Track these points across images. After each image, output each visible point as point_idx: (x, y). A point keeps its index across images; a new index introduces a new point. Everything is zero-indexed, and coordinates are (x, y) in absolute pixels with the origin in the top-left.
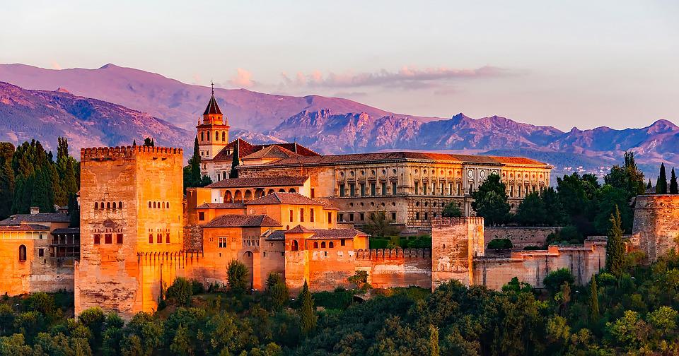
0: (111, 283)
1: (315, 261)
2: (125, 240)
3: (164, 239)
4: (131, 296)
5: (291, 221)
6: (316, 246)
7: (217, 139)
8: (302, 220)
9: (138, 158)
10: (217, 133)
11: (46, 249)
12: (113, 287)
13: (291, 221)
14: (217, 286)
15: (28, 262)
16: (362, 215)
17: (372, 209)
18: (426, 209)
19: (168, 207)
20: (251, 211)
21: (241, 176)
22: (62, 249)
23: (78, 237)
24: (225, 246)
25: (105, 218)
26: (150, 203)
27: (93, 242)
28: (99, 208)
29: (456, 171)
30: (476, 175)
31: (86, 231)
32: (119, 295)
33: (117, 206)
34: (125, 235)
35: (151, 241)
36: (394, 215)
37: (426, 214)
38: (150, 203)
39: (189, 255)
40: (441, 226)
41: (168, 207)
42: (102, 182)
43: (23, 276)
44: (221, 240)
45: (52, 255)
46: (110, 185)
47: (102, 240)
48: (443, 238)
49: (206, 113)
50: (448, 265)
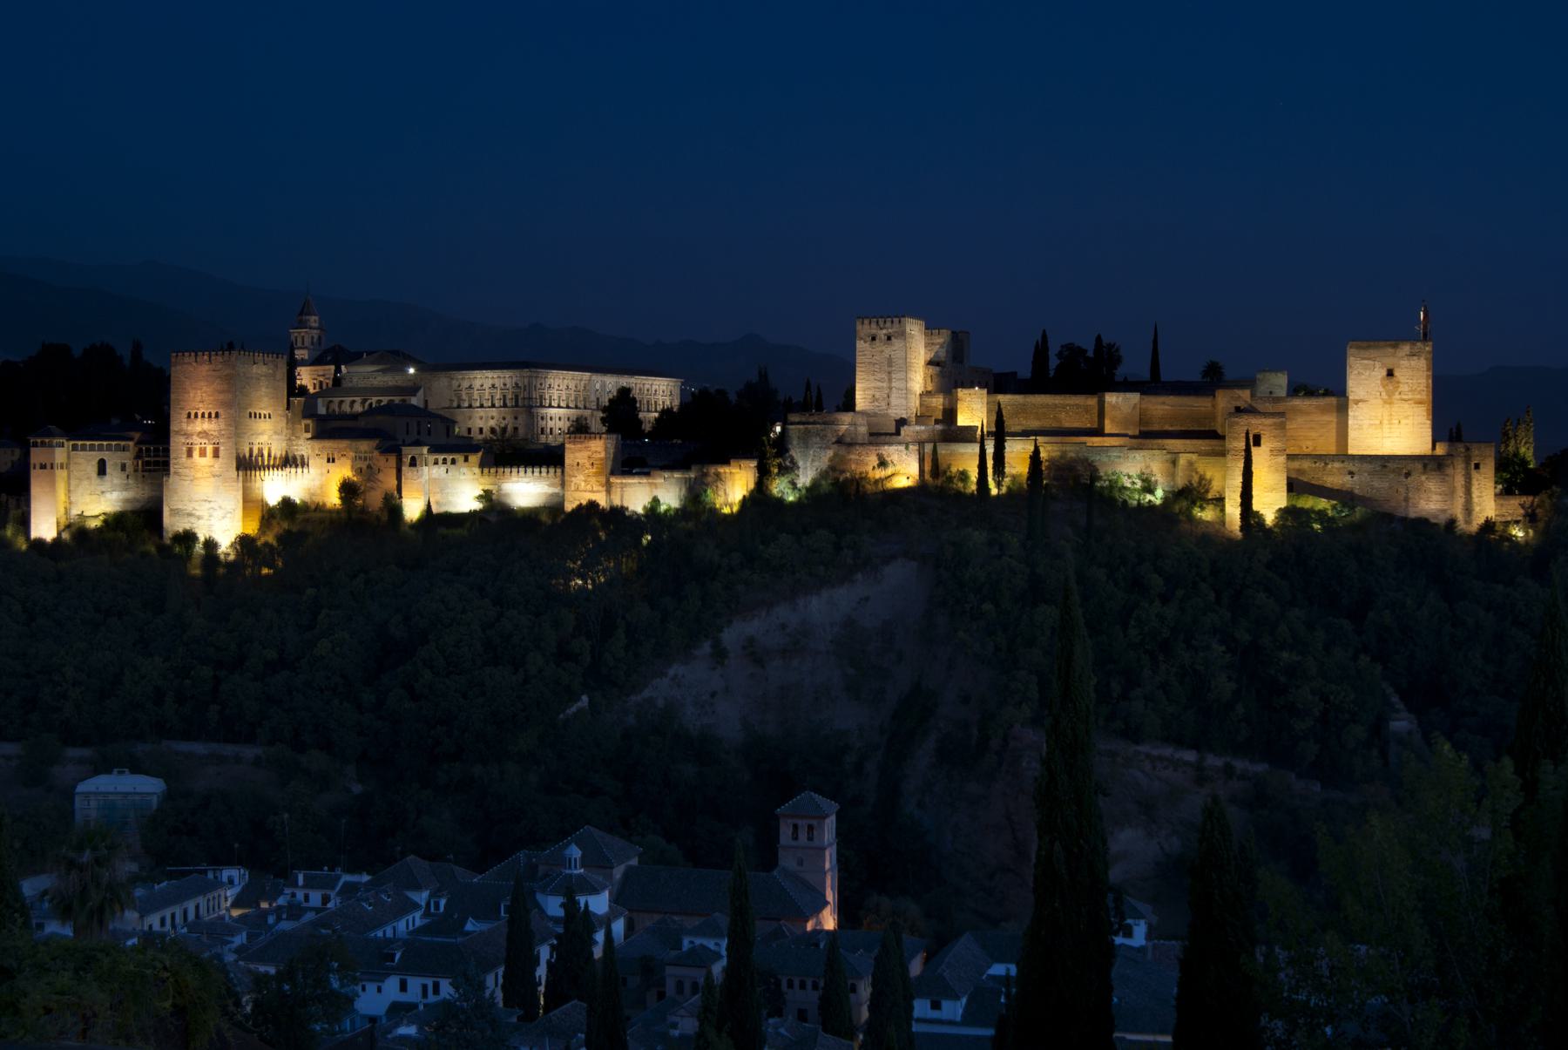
0: (206, 501)
1: (435, 479)
2: (221, 453)
4: (229, 515)
5: (407, 433)
6: (436, 463)
8: (419, 433)
11: (129, 463)
12: (208, 505)
13: (407, 433)
14: (324, 505)
15: (107, 477)
16: (481, 430)
17: (492, 423)
18: (550, 424)
19: (270, 417)
21: (346, 384)
22: (148, 463)
23: (167, 451)
24: (333, 461)
26: (250, 414)
27: (185, 456)
29: (583, 382)
30: (603, 385)
31: (177, 444)
32: (215, 514)
33: (213, 415)
34: (222, 448)
35: (251, 455)
36: (516, 429)
37: (551, 429)
38: (250, 414)
39: (293, 470)
40: (574, 443)
41: (270, 417)
42: (195, 389)
43: (103, 492)
44: (328, 454)
45: (136, 471)
46: (205, 392)
47: (196, 454)
48: (577, 454)
49: (301, 314)
50: (583, 484)
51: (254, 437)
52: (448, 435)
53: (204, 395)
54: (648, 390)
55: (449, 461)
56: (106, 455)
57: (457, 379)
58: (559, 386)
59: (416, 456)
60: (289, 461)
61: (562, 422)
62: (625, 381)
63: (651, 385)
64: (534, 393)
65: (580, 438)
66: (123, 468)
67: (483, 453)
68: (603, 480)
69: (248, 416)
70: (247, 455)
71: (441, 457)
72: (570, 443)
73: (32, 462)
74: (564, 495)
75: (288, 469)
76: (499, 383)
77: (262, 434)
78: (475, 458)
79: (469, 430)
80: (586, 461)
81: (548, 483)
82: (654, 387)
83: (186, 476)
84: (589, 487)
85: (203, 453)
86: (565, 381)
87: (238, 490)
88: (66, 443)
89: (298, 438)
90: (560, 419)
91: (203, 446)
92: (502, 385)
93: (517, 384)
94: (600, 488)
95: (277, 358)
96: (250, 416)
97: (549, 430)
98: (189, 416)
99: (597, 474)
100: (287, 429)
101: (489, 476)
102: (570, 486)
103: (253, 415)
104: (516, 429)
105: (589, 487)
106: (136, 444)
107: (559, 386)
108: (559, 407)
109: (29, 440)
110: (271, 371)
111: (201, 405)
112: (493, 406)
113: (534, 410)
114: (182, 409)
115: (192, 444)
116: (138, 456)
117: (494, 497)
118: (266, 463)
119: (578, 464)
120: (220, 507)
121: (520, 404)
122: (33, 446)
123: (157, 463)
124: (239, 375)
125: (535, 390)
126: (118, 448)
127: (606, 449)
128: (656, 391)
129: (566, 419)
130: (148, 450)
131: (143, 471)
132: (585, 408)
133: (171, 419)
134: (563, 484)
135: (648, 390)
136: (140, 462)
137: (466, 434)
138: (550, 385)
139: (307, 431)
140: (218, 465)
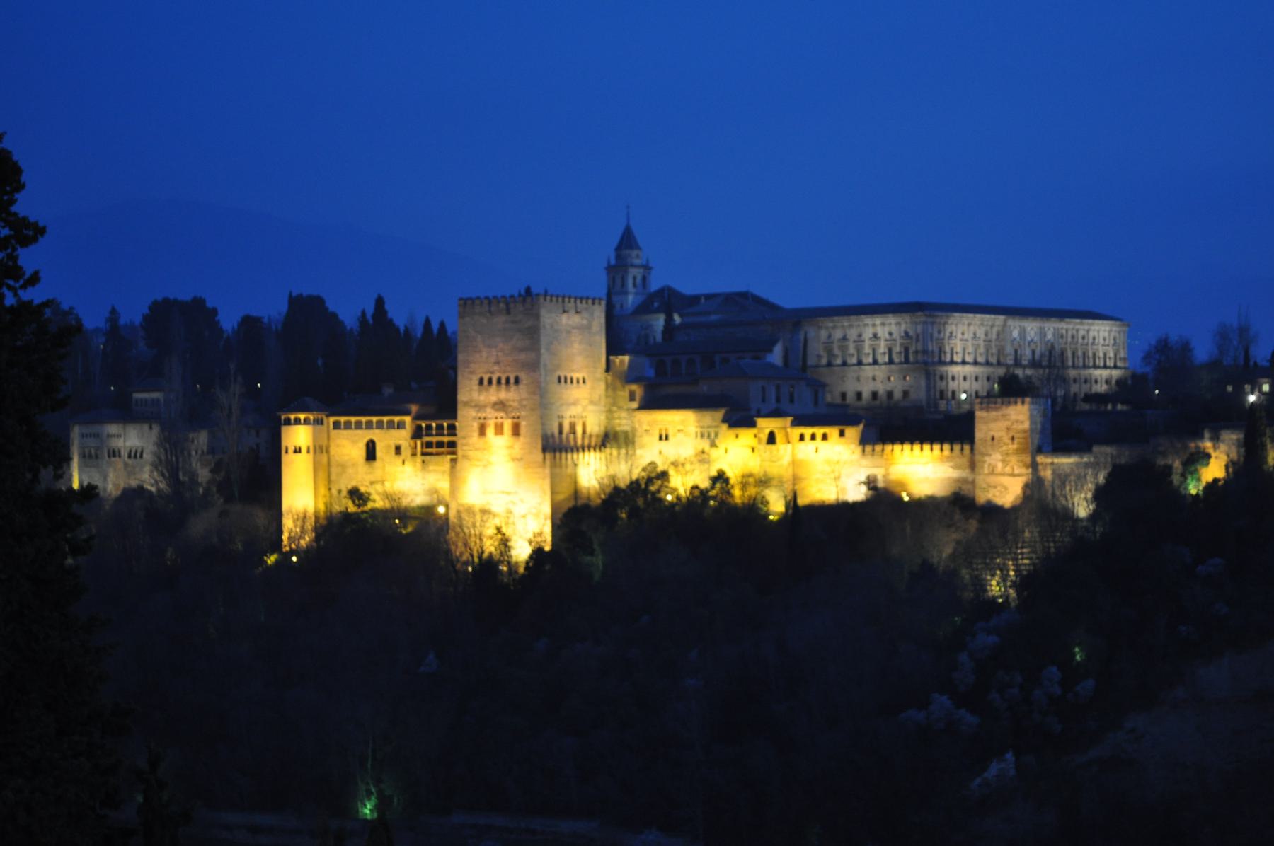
0: (503, 492)
2: (523, 430)
3: (579, 430)
5: (763, 401)
7: (635, 285)
8: (778, 400)
9: (543, 312)
10: (635, 278)
13: (763, 401)
15: (378, 463)
18: (952, 385)
19: (584, 382)
20: (705, 388)
22: (429, 445)
23: (452, 430)
24: (667, 438)
25: (494, 399)
27: (476, 434)
28: (486, 382)
30: (1023, 332)
33: (512, 380)
34: (523, 423)
35: (561, 432)
39: (615, 452)
40: (988, 409)
41: (584, 382)
42: (489, 346)
44: (660, 430)
45: (414, 454)
47: (490, 431)
48: (992, 425)
50: (1000, 465)
51: (564, 407)
52: (816, 403)
53: (500, 354)
54: (1083, 338)
55: (819, 437)
56: (375, 435)
57: (827, 328)
58: (963, 334)
59: (776, 431)
60: (607, 439)
61: (968, 383)
62: (1051, 328)
63: (1088, 331)
64: (930, 344)
65: (995, 403)
66: (398, 450)
67: (865, 426)
68: (1028, 459)
69: (556, 381)
70: (556, 432)
71: (808, 431)
72: (981, 409)
73: (284, 444)
74: (973, 482)
75: (608, 450)
76: (882, 332)
77: (575, 403)
78: (853, 433)
79: (844, 395)
80: (1003, 434)
81: (951, 464)
82: (1091, 334)
83: (478, 460)
84: (1008, 469)
85: (499, 430)
86: (972, 328)
87: (544, 479)
88: (325, 420)
89: (620, 408)
90: (965, 379)
91: (499, 420)
92: (887, 336)
93: (906, 333)
94: (1024, 471)
95: (593, 304)
96: (559, 381)
97: (950, 394)
98: (481, 382)
99: (1018, 452)
100: (607, 396)
101: (873, 455)
102: (982, 467)
103: (563, 380)
104: (906, 393)
105: (1008, 469)
106: (417, 417)
107: (963, 334)
108: (964, 363)
109: (280, 417)
110: (585, 322)
111: (496, 368)
112: (875, 362)
113: (931, 368)
114: (472, 373)
115: (485, 419)
116: (417, 434)
117: (881, 484)
118: (579, 442)
119: (993, 439)
120: (522, 501)
121: (911, 358)
122: (285, 424)
123: (440, 445)
124: (544, 327)
125: (932, 340)
126: (391, 425)
127: (1032, 417)
128: (1094, 338)
129: (973, 379)
130: (429, 427)
131: (423, 454)
132: (999, 363)
133: (459, 386)
134: (973, 466)
135: (1083, 338)
136: (419, 443)
137: (838, 401)
138: (951, 333)
139: (632, 398)
140: (519, 446)
